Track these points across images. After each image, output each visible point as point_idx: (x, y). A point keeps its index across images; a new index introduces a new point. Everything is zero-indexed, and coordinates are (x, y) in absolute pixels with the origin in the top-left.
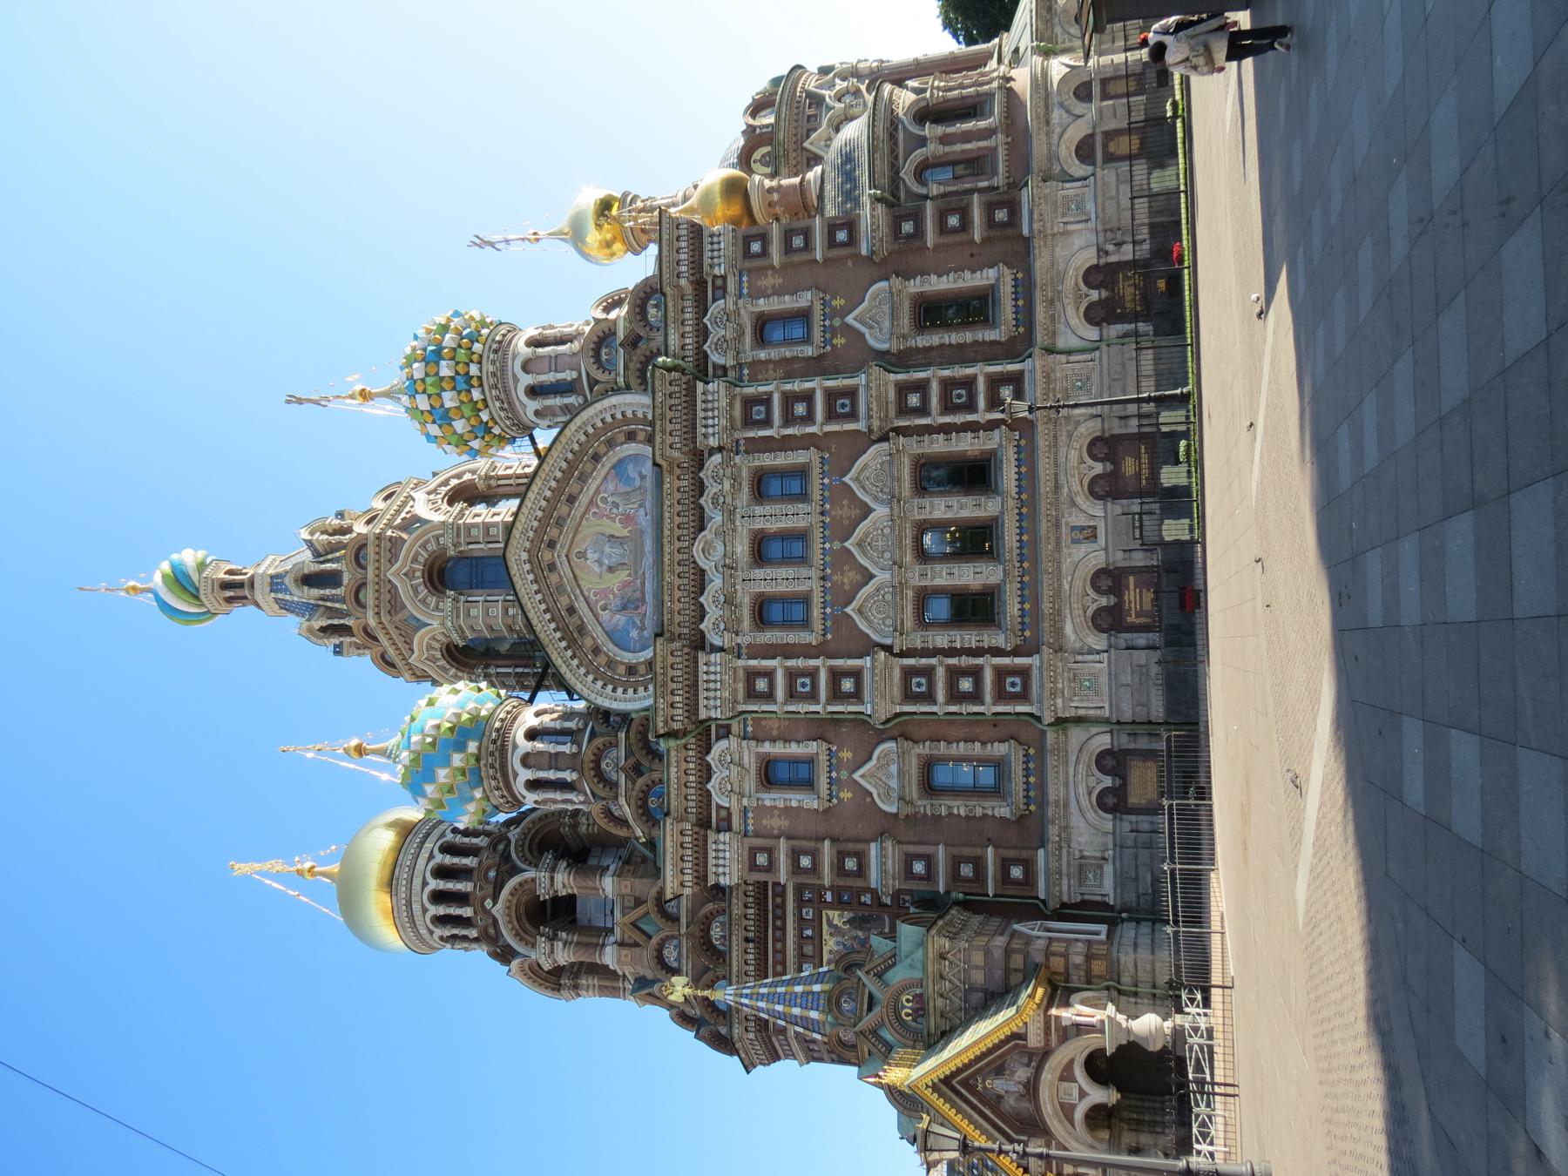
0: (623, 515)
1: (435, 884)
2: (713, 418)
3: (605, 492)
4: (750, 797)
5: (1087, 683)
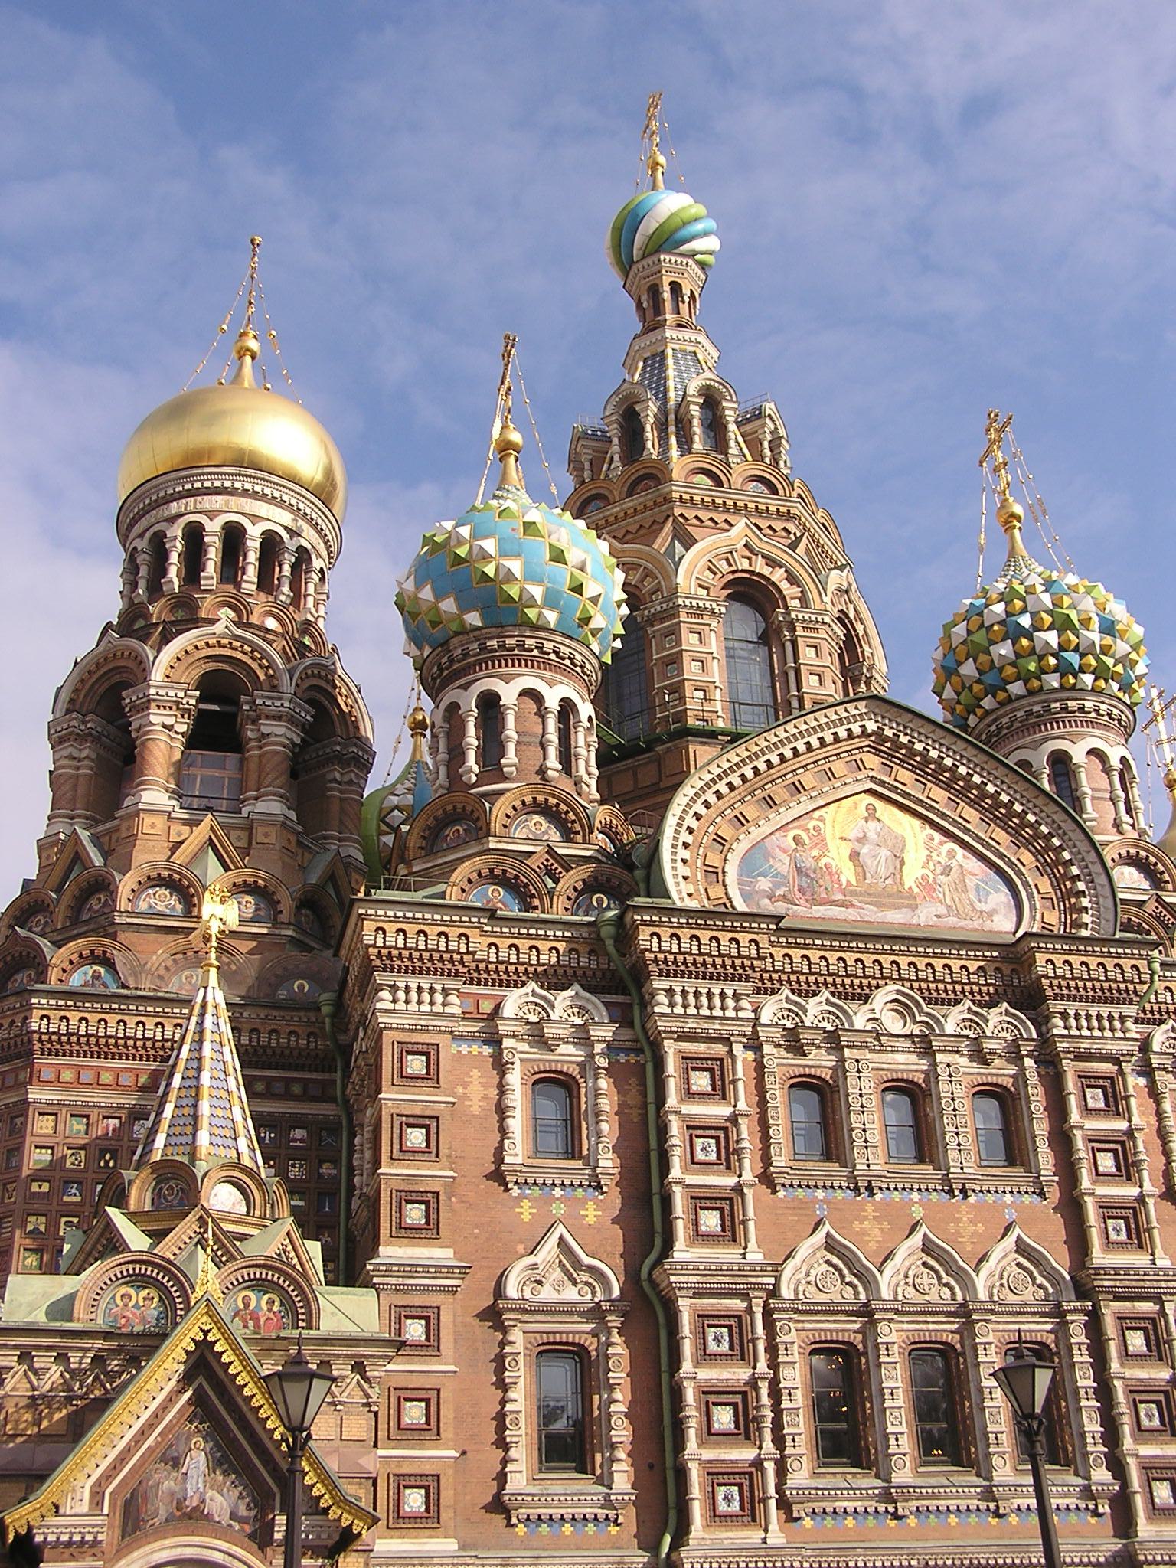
1: (254, 533)
3: (964, 856)
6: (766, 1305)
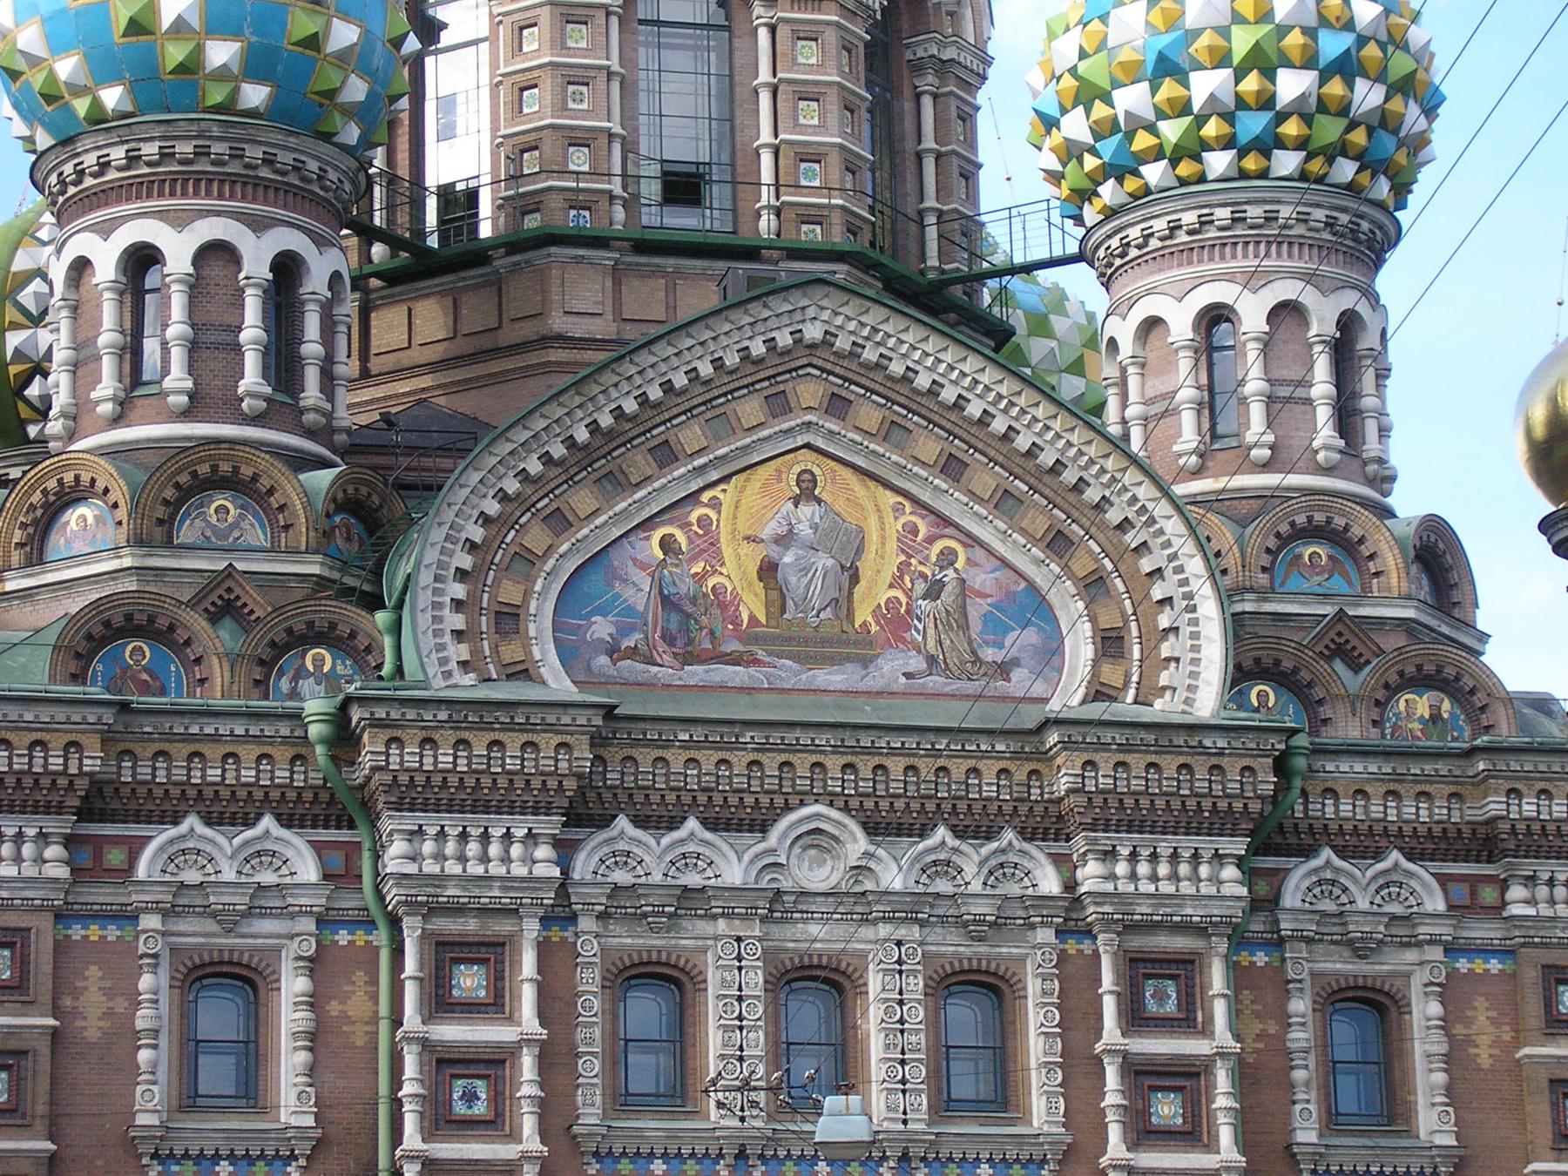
0: (908, 611)
2: (1154, 878)
3: (969, 561)
4: (164, 934)
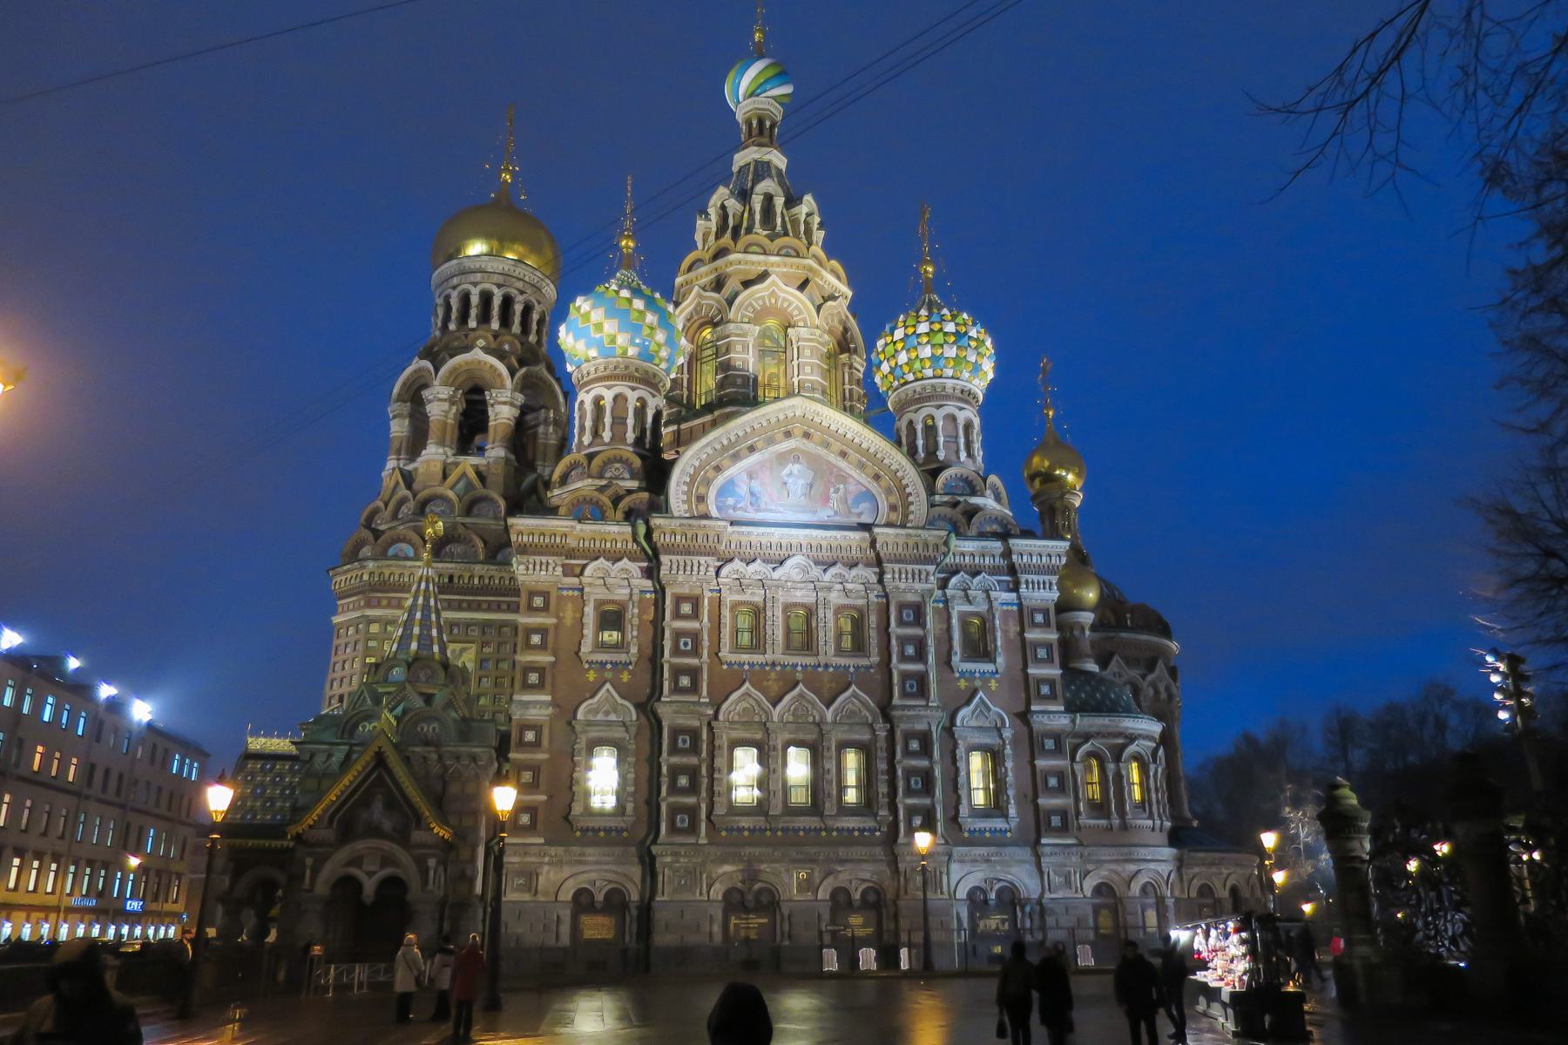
5: (683, 882)
6: (709, 724)
